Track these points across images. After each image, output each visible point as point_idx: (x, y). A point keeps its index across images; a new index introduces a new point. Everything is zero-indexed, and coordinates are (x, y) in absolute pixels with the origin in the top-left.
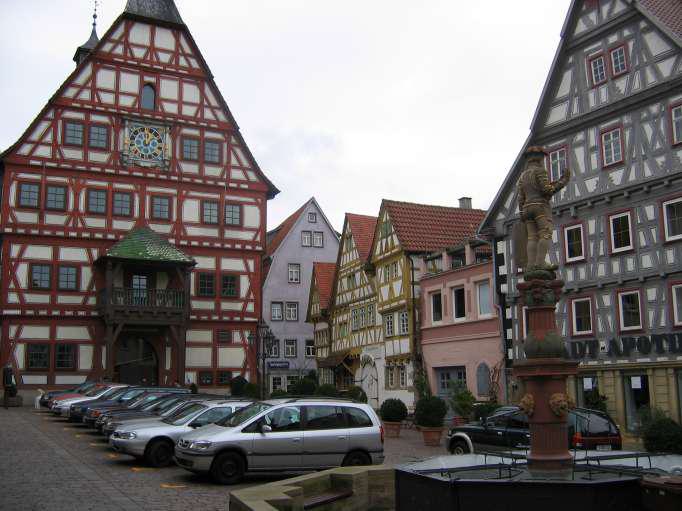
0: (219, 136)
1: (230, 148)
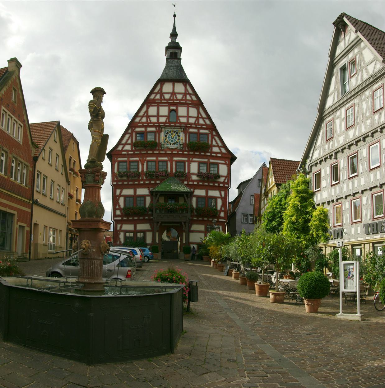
0: (207, 131)
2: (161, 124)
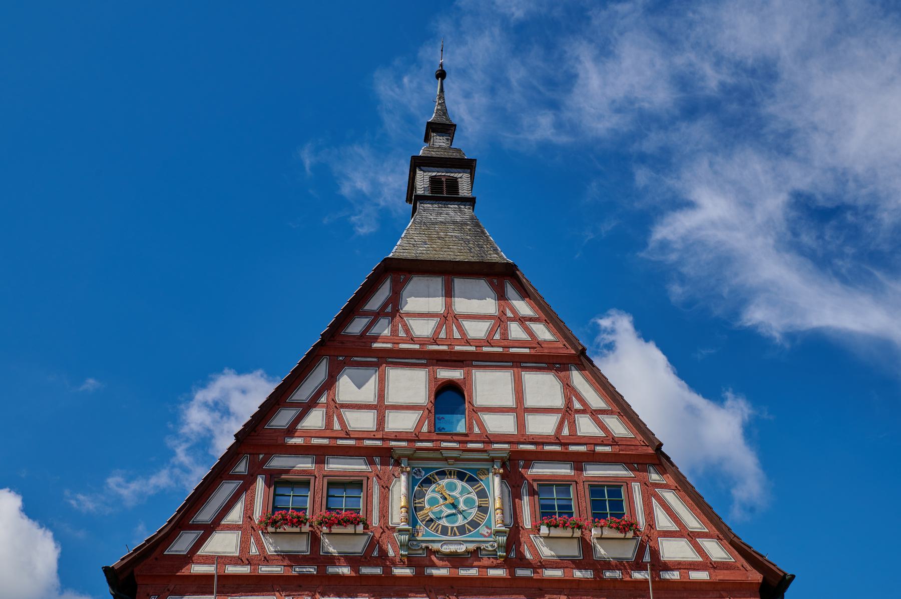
0: (619, 472)
1: (649, 491)
2: (393, 443)
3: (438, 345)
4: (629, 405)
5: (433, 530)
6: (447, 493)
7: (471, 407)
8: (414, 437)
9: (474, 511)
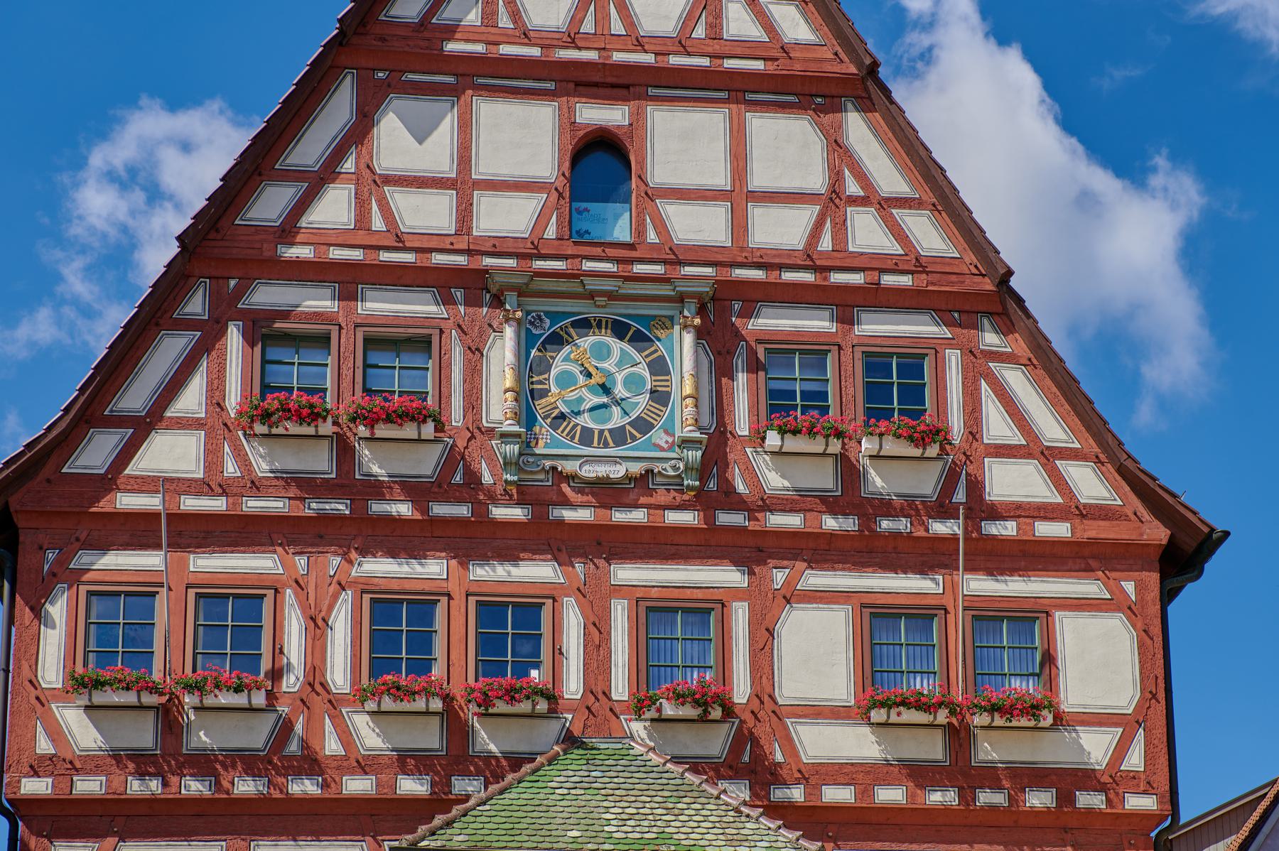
0: (923, 327)
2: (488, 261)
3: (580, 48)
4: (955, 189)
5: (564, 435)
6: (592, 363)
7: (643, 187)
8: (530, 250)
9: (643, 400)
